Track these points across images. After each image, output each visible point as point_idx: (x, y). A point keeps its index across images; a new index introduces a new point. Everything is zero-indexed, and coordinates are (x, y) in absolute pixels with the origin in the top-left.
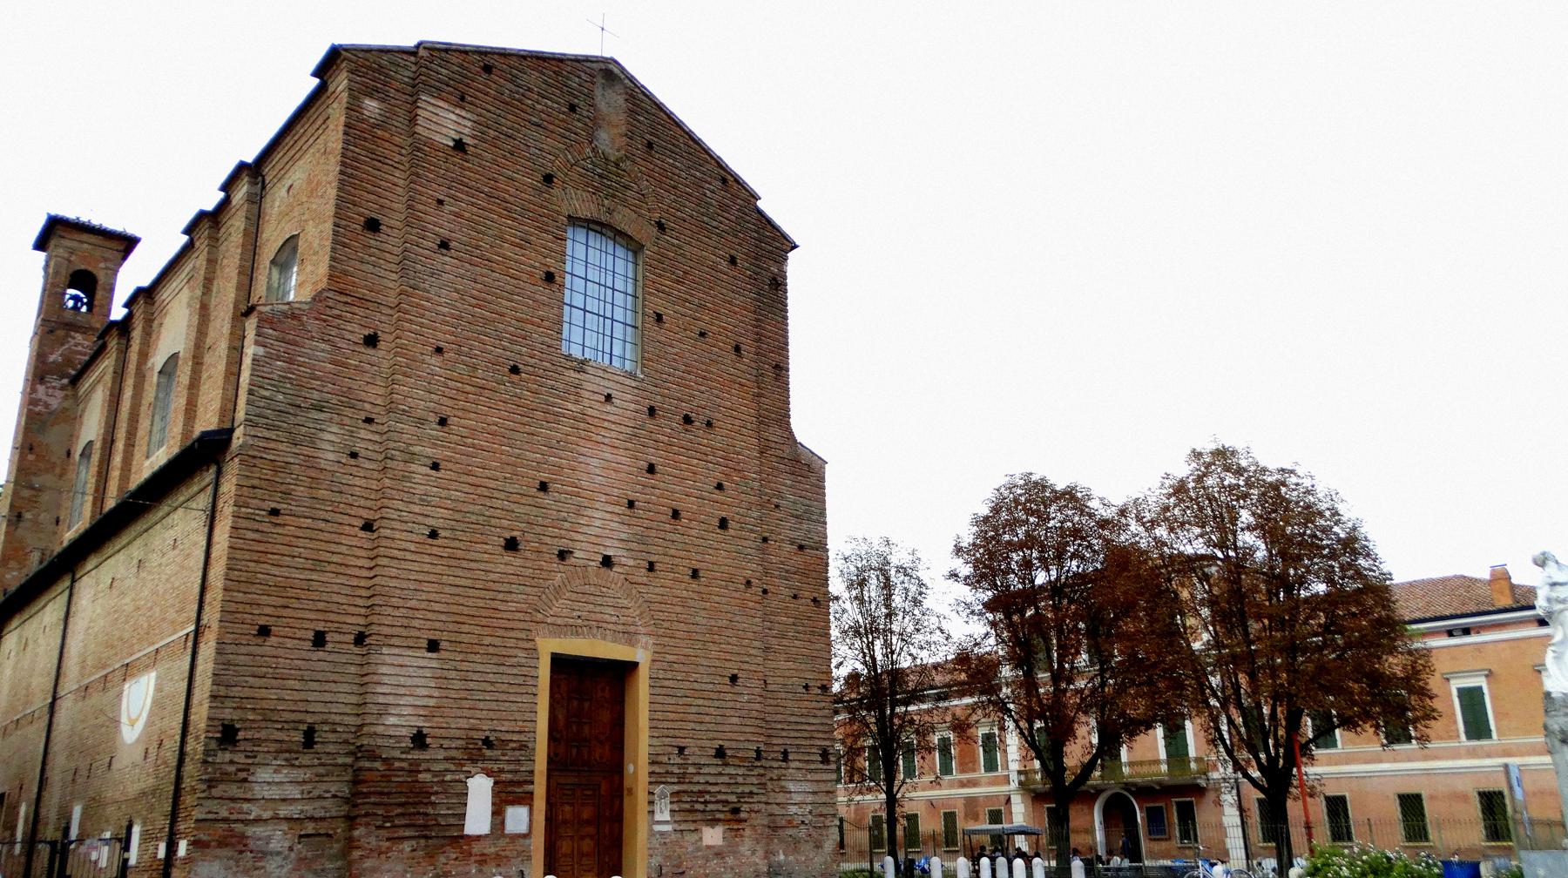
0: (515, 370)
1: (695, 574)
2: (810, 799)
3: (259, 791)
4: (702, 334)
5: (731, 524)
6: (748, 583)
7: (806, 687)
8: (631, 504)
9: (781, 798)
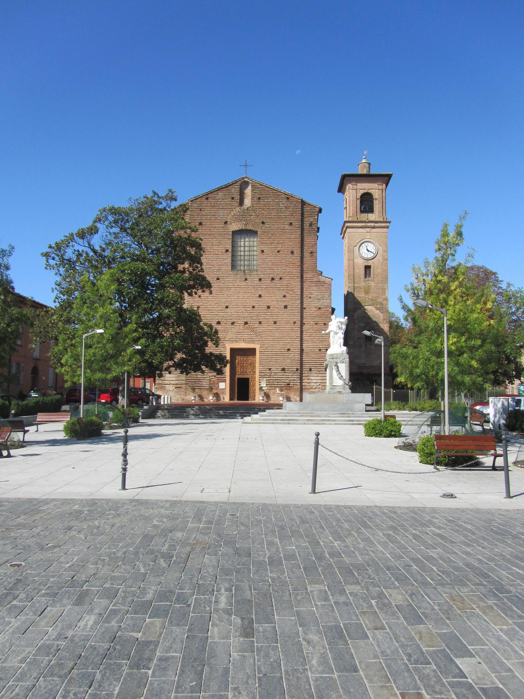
0: (218, 279)
1: (275, 323)
2: (320, 381)
3: (167, 379)
4: (278, 252)
5: (289, 306)
6: (295, 323)
7: (320, 350)
8: (253, 307)
9: (308, 381)
